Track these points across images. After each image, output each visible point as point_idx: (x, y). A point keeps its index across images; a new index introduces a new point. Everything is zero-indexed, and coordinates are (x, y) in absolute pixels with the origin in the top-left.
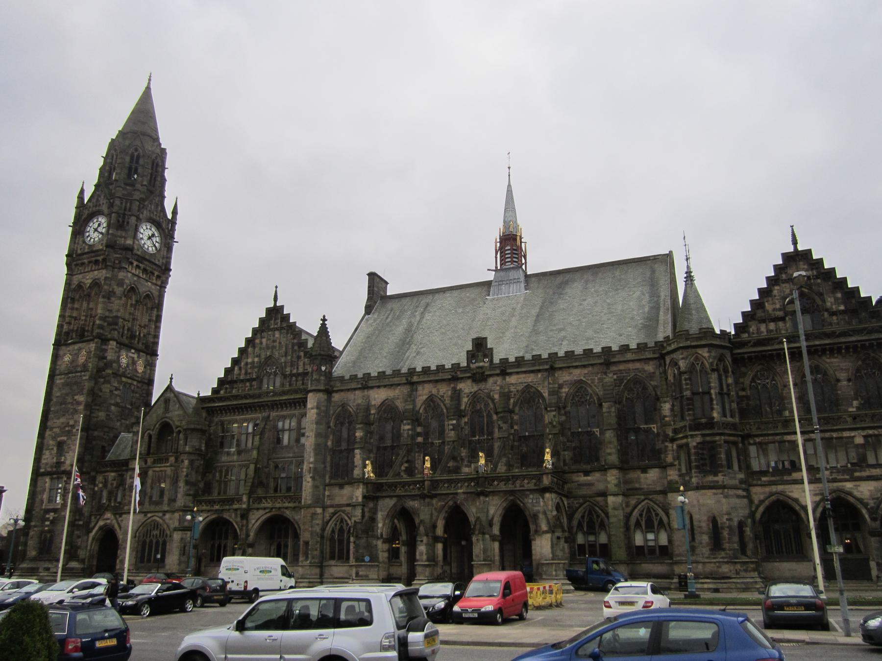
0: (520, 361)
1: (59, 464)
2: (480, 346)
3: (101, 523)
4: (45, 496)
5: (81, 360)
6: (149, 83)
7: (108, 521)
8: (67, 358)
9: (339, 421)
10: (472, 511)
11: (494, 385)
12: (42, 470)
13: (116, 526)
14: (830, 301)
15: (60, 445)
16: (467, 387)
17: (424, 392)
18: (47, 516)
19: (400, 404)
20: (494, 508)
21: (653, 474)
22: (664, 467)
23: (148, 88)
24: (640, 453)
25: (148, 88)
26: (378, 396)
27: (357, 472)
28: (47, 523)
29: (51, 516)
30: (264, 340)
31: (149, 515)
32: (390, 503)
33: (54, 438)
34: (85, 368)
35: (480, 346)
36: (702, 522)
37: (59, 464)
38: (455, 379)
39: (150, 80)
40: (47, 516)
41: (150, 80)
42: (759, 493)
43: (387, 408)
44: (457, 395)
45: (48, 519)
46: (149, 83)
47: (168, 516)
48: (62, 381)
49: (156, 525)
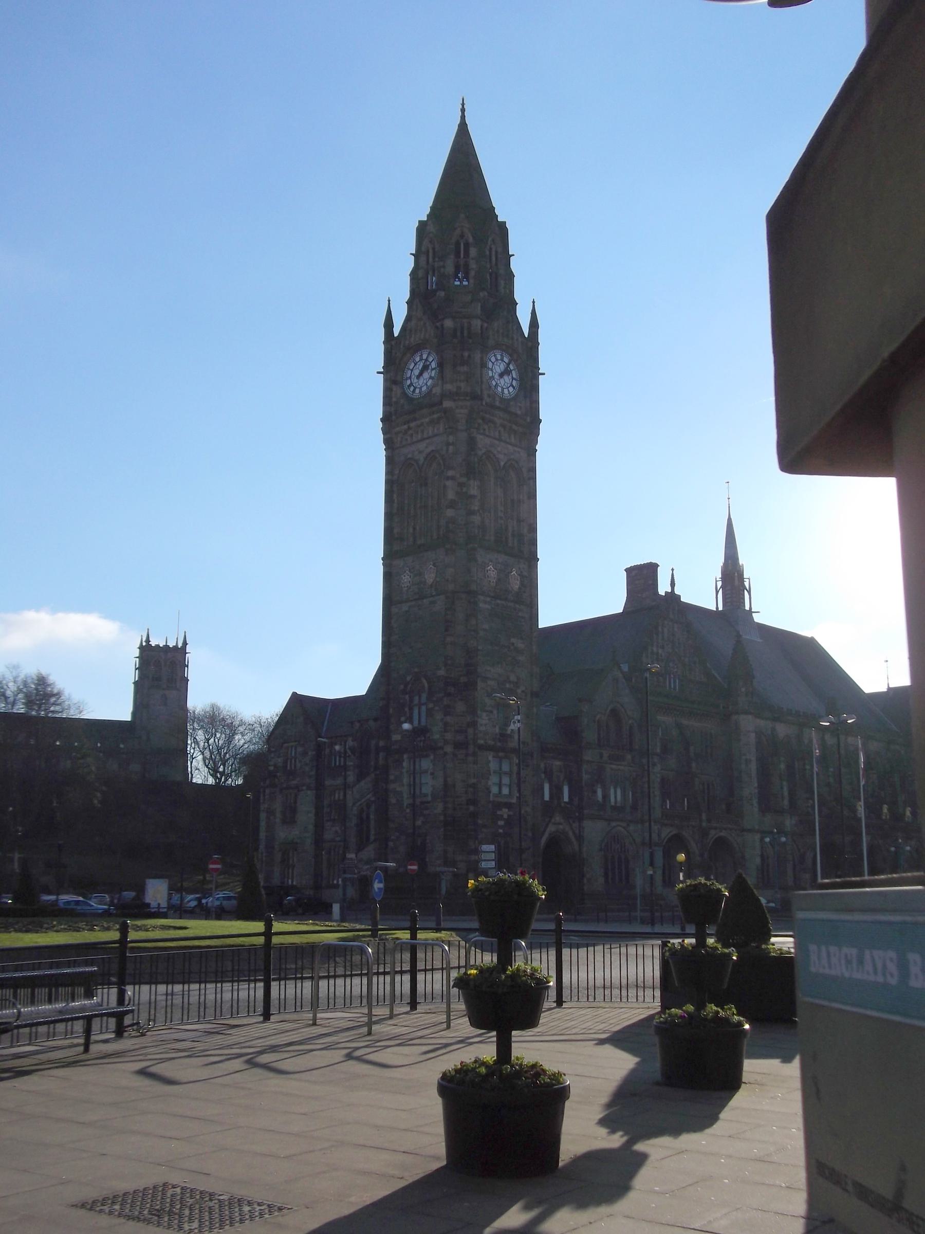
3: (551, 828)
6: (463, 117)
7: (561, 827)
12: (481, 742)
13: (571, 834)
18: (499, 813)
23: (463, 129)
25: (463, 129)
28: (501, 823)
29: (505, 812)
31: (614, 824)
33: (489, 695)
39: (463, 110)
40: (499, 813)
41: (463, 110)
45: (501, 817)
46: (463, 117)
47: (632, 828)
48: (489, 607)
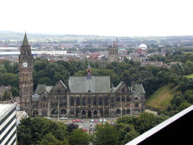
0: (94, 93)
1: (26, 102)
2: (89, 91)
4: (24, 106)
5: (27, 86)
8: (24, 86)
9: (72, 99)
10: (91, 111)
11: (91, 96)
14: (126, 89)
15: (26, 99)
16: (88, 96)
17: (83, 96)
19: (79, 97)
20: (94, 111)
21: (107, 106)
22: (109, 106)
23: (25, 34)
24: (106, 104)
25: (25, 34)
26: (77, 96)
27: (75, 105)
29: (26, 109)
30: (58, 86)
32: (82, 110)
34: (28, 88)
35: (89, 91)
36: (112, 111)
37: (26, 102)
38: (87, 95)
42: (117, 108)
43: (78, 97)
44: (87, 96)
49: (44, 110)
